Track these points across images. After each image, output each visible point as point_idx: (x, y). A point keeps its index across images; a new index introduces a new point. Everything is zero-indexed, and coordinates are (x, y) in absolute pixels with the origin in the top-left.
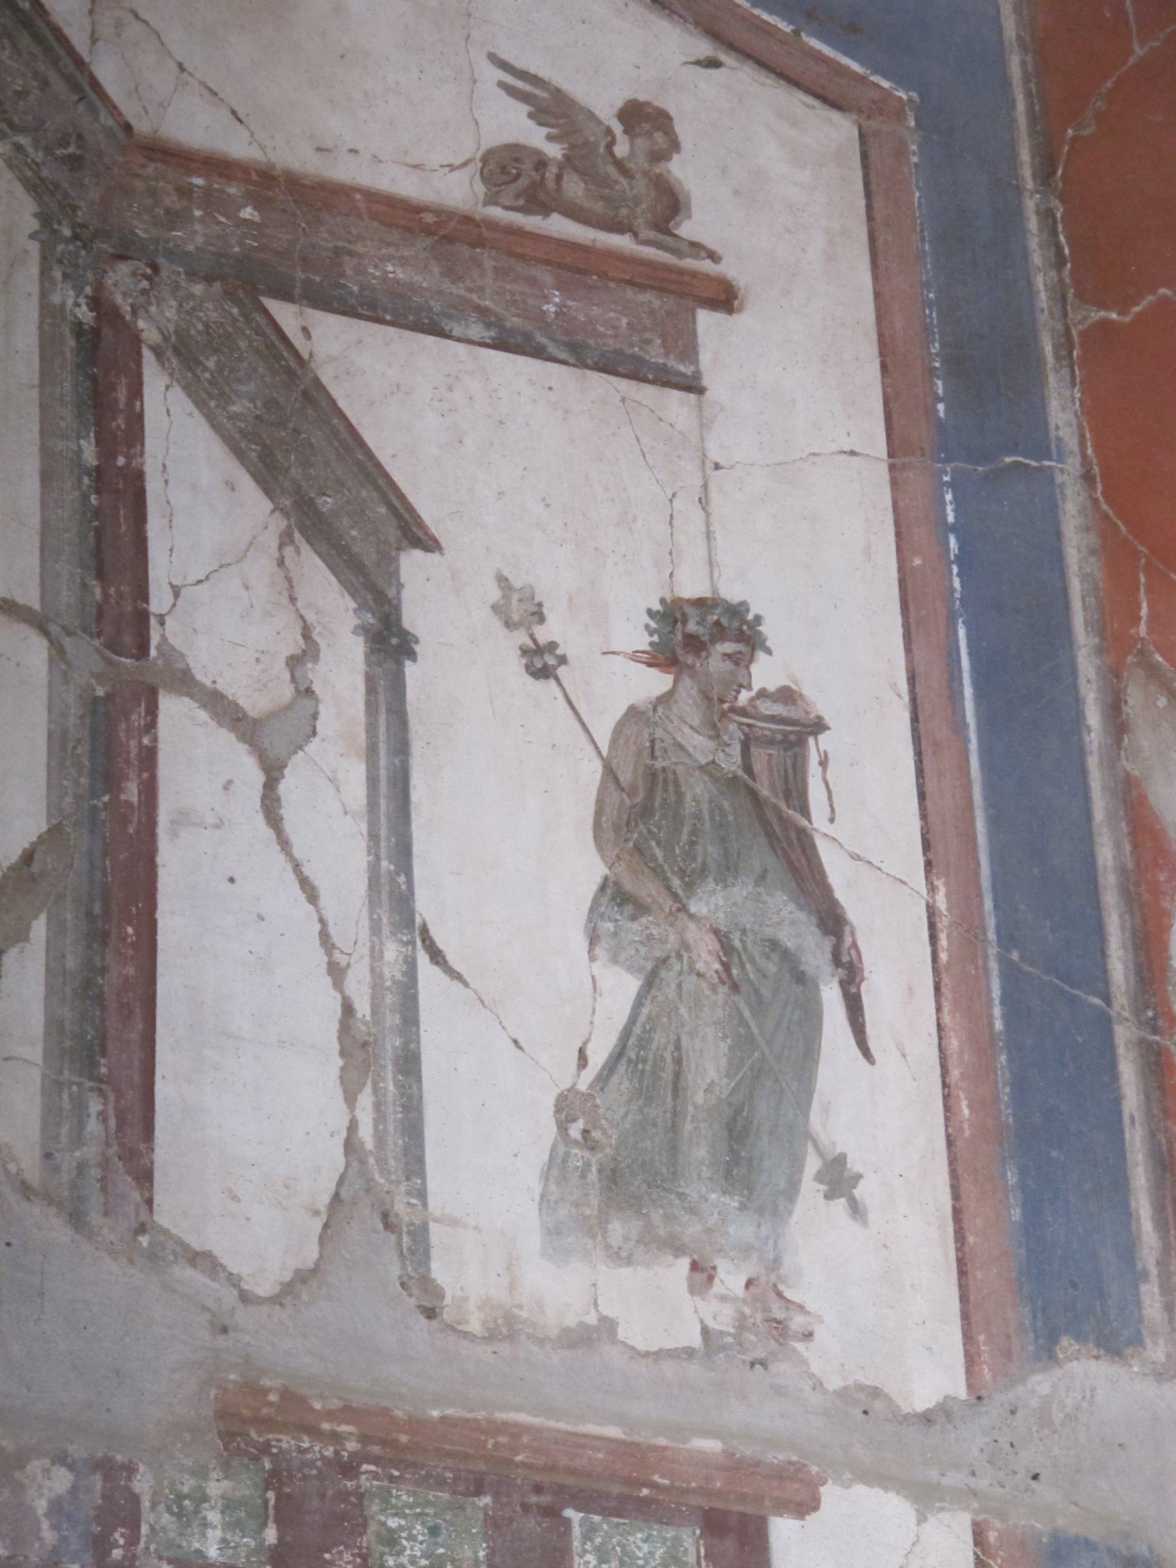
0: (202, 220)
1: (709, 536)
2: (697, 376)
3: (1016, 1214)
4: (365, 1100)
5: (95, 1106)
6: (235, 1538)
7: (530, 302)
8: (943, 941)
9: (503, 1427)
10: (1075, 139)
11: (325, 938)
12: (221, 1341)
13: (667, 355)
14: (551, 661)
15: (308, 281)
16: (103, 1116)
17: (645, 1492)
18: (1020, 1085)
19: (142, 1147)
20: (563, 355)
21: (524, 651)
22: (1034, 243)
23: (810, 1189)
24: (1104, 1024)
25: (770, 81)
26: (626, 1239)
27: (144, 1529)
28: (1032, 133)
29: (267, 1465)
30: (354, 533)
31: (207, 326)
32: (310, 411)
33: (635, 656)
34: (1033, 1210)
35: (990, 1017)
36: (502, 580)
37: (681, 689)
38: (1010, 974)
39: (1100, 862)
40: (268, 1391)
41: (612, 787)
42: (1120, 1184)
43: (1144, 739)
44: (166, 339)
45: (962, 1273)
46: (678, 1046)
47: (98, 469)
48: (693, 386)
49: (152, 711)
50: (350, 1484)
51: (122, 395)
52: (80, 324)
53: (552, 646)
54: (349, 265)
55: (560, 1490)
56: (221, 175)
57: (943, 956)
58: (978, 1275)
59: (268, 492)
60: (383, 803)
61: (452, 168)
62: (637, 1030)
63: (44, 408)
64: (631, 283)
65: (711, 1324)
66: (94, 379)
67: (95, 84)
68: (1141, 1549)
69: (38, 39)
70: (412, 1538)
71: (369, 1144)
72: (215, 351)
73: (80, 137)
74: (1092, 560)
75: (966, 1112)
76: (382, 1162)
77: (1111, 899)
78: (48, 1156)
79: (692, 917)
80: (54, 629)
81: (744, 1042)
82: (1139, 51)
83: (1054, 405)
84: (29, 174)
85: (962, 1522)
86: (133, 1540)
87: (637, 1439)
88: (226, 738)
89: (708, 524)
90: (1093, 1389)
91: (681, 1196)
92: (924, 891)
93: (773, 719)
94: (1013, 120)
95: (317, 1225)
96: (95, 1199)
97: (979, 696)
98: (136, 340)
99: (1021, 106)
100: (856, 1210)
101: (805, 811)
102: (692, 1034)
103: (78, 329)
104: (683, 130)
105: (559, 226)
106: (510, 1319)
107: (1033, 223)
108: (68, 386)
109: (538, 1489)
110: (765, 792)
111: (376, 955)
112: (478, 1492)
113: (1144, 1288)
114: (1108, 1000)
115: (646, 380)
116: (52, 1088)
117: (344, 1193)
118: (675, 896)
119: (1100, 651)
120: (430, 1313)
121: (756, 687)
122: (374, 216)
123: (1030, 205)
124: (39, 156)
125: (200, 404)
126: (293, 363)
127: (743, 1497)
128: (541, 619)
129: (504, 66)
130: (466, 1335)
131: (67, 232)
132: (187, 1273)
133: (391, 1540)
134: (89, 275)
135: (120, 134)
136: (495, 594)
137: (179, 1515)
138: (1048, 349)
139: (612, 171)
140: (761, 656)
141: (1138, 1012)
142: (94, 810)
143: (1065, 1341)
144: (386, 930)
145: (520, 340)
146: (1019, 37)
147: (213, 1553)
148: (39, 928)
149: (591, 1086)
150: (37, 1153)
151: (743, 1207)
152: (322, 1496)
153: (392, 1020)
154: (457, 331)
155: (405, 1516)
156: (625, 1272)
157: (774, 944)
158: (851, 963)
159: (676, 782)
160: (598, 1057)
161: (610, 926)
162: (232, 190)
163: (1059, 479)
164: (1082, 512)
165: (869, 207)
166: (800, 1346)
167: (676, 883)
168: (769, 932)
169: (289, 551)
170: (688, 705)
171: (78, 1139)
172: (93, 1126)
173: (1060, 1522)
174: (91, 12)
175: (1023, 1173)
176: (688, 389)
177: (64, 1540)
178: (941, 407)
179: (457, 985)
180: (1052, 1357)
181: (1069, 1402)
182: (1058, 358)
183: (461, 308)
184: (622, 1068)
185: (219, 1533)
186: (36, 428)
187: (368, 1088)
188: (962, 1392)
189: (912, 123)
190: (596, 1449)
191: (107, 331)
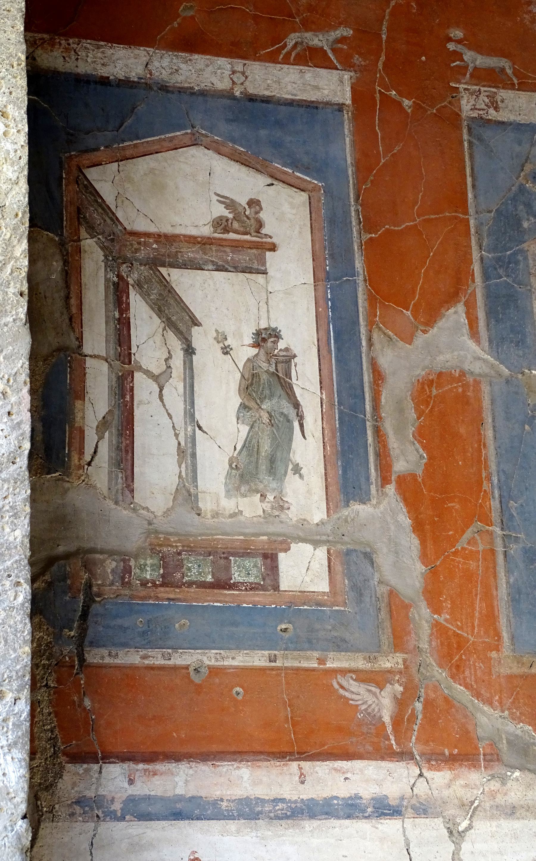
0: (143, 250)
1: (268, 311)
2: (266, 269)
3: (340, 472)
4: (183, 466)
5: (120, 475)
6: (153, 573)
7: (224, 257)
8: (324, 407)
9: (215, 540)
10: (365, 188)
11: (173, 427)
12: (150, 527)
13: (258, 265)
14: (228, 350)
15: (169, 261)
16: (122, 478)
17: (249, 551)
18: (342, 439)
19: (131, 484)
20: (232, 270)
21: (222, 348)
22: (353, 219)
23: (290, 472)
24: (364, 421)
25: (286, 186)
26: (245, 491)
27: (133, 573)
28: (354, 189)
29: (161, 555)
30: (181, 325)
31: (145, 277)
32: (170, 295)
33: (249, 346)
34: (345, 471)
35: (335, 424)
36: (216, 331)
37: (261, 353)
38: (341, 412)
39: (364, 381)
40: (161, 538)
41: (243, 380)
43: (377, 346)
44: (135, 282)
45: (326, 488)
46: (258, 442)
47: (119, 318)
48: (265, 273)
49: (133, 377)
50: (180, 557)
51: (124, 299)
52: (114, 282)
53: (229, 345)
54: (179, 254)
55: (229, 553)
56: (148, 237)
57: (324, 410)
58: (330, 488)
59: (160, 318)
60: (187, 392)
61: (205, 225)
62: (248, 439)
63: (106, 305)
64: (250, 248)
65: (265, 509)
66: (118, 295)
67: (117, 219)
68: (368, 550)
69: (103, 209)
70: (194, 568)
71: (184, 476)
72: (147, 283)
73: (114, 233)
74: (365, 302)
75: (329, 448)
76: (187, 480)
77: (367, 389)
78: (109, 489)
79: (262, 409)
80: (109, 360)
81: (274, 438)
82: (383, 161)
83: (357, 262)
84: (101, 245)
85: (324, 549)
86: (130, 576)
87: (247, 538)
88: (150, 381)
89: (268, 308)
90: (358, 512)
91: (258, 479)
92: (320, 395)
93: (283, 356)
94: (349, 186)
95: (172, 497)
96: (120, 498)
97: (335, 343)
98: (128, 284)
99: (351, 182)
100: (301, 476)
101: (291, 379)
102: (262, 439)
103: (114, 284)
104: (263, 205)
105: (232, 236)
106: (217, 514)
107: (353, 214)
108: (111, 298)
109: (224, 553)
110: (281, 375)
111: (186, 430)
112: (209, 556)
113: (371, 486)
114: (365, 416)
115: (253, 273)
116: (110, 473)
117: (178, 488)
118: (258, 404)
119: (366, 326)
120: (199, 515)
121: (279, 349)
122: (186, 241)
123: (352, 209)
124: (104, 240)
125: (144, 298)
126: (166, 283)
127: (272, 549)
128: (226, 339)
129: (218, 195)
130: (208, 519)
131: (111, 258)
132: (142, 512)
133: (189, 569)
134: (116, 269)
135: (123, 230)
136: (215, 335)
137: (141, 569)
138: (356, 247)
139: (245, 219)
140: (280, 340)
141: (373, 417)
142: (119, 404)
143: (351, 502)
144: (188, 423)
145: (222, 268)
146: (351, 163)
147: (148, 577)
148: (107, 434)
149: (237, 455)
150: (107, 489)
151: (273, 479)
152: (173, 561)
153: (189, 445)
154: (206, 268)
155: (192, 563)
156: (245, 499)
157: (282, 413)
158: (301, 415)
159: (259, 376)
160: (239, 448)
161: (242, 414)
162: (151, 241)
163: (357, 282)
164: (363, 290)
165: (311, 217)
166: (287, 511)
167: (258, 401)
168: (281, 410)
169: (165, 332)
170: (262, 357)
171: (116, 484)
172: (120, 480)
173: (349, 546)
174: (116, 200)
175: (342, 462)
176: (264, 273)
177: (114, 578)
178: (328, 268)
179: (205, 434)
180: (348, 506)
181: (352, 516)
182: (358, 249)
183: (206, 262)
184: (244, 449)
185: (150, 572)
186: (104, 310)
187: (184, 462)
188: (325, 517)
189: (322, 192)
190: (237, 542)
191: (121, 283)
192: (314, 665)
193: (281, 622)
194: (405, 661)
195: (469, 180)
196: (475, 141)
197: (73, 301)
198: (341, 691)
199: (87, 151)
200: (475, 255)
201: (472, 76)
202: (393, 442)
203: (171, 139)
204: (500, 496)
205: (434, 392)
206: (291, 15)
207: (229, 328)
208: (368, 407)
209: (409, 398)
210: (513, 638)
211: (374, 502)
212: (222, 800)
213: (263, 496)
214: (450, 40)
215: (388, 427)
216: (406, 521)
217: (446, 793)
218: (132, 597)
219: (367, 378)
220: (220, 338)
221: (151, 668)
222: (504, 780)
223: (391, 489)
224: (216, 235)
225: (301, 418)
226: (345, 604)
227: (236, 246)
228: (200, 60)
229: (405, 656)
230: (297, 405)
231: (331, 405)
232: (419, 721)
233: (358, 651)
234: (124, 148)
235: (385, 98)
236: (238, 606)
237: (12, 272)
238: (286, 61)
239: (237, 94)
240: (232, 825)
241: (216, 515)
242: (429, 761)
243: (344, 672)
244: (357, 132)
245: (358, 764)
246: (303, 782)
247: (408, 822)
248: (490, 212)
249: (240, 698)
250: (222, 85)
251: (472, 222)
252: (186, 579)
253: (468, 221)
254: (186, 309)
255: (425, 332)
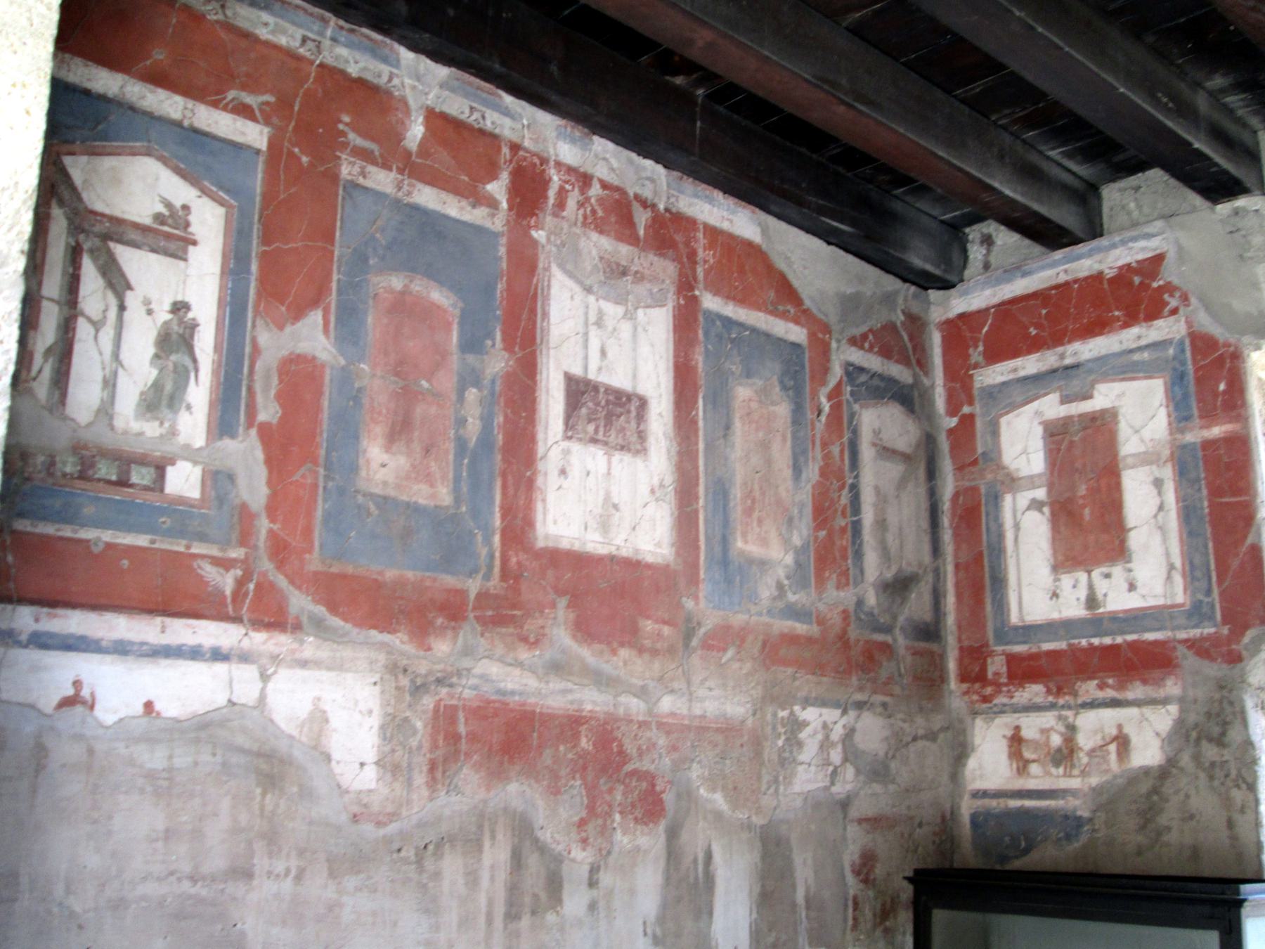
24: (241, 380)
38: (226, 371)
42: (239, 410)
48: (185, 260)
81: (175, 383)
98: (82, 250)
100: (191, 413)
105: (166, 228)
157: (183, 366)
162: (105, 220)
170: (175, 322)
183: (144, 244)
192: (182, 549)
193: (162, 516)
194: (246, 553)
195: (338, 224)
196: (347, 197)
197: (39, 254)
198: (199, 571)
199: (66, 142)
200: (335, 277)
201: (352, 151)
202: (260, 399)
203: (132, 147)
204: (327, 448)
205: (293, 368)
206: (232, 76)
207: (154, 295)
208: (246, 370)
209: (275, 369)
210: (321, 546)
211: (240, 439)
212: (102, 639)
213: (162, 424)
214: (341, 122)
215: (258, 387)
216: (260, 455)
217: (263, 648)
218: (54, 484)
219: (248, 349)
220: (147, 302)
221: (61, 538)
222: (302, 642)
223: (253, 432)
224: (155, 226)
225: (197, 370)
226: (209, 509)
227: (168, 236)
228: (162, 94)
229: (246, 550)
230: (195, 361)
231: (220, 366)
232: (250, 597)
233: (213, 543)
234: (95, 147)
235: (291, 155)
236: (133, 502)
237: (18, 234)
238: (225, 109)
239: (186, 123)
240: (108, 658)
241: (125, 433)
242: (253, 624)
243: (203, 557)
244: (265, 172)
245: (203, 623)
246: (163, 632)
247: (234, 666)
248: (349, 248)
249: (126, 567)
250: (175, 114)
251: (336, 253)
252: (97, 476)
253: (332, 253)
254: (123, 275)
255: (293, 324)
